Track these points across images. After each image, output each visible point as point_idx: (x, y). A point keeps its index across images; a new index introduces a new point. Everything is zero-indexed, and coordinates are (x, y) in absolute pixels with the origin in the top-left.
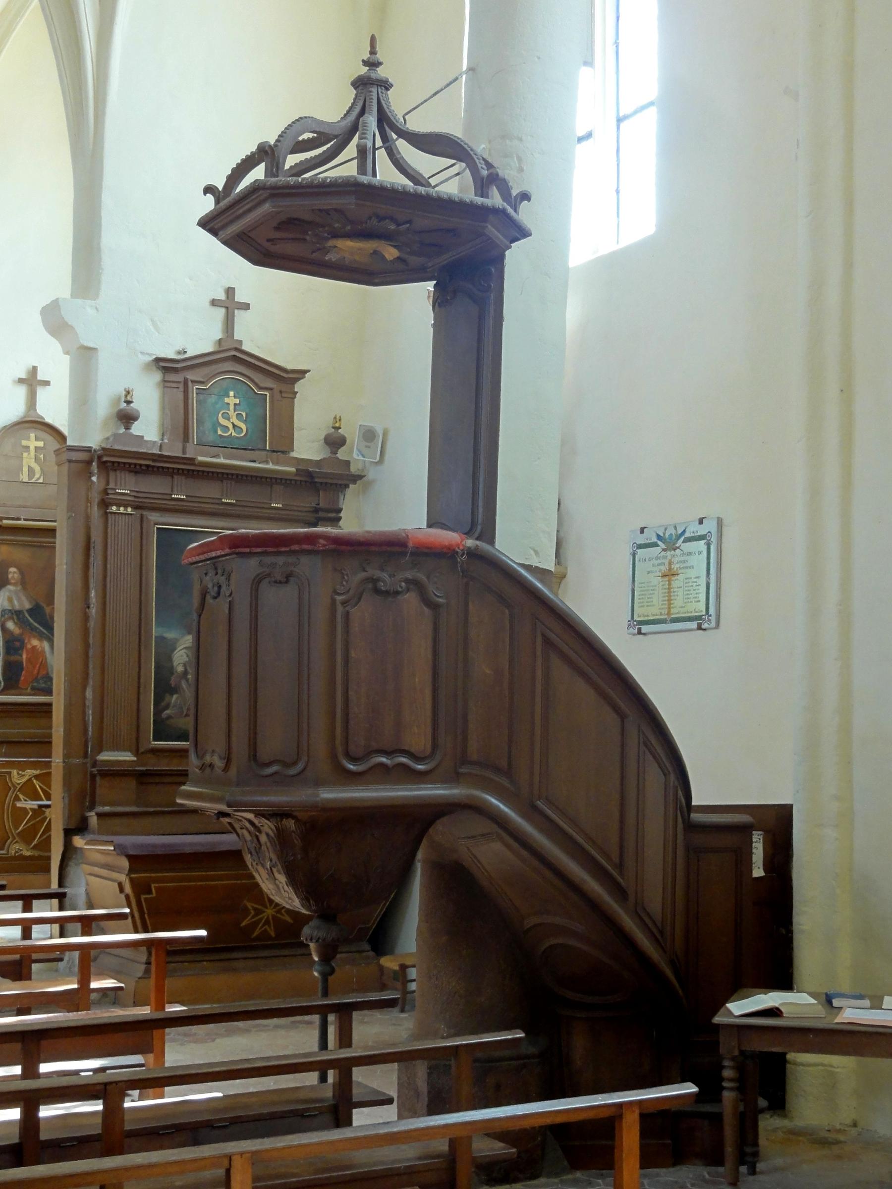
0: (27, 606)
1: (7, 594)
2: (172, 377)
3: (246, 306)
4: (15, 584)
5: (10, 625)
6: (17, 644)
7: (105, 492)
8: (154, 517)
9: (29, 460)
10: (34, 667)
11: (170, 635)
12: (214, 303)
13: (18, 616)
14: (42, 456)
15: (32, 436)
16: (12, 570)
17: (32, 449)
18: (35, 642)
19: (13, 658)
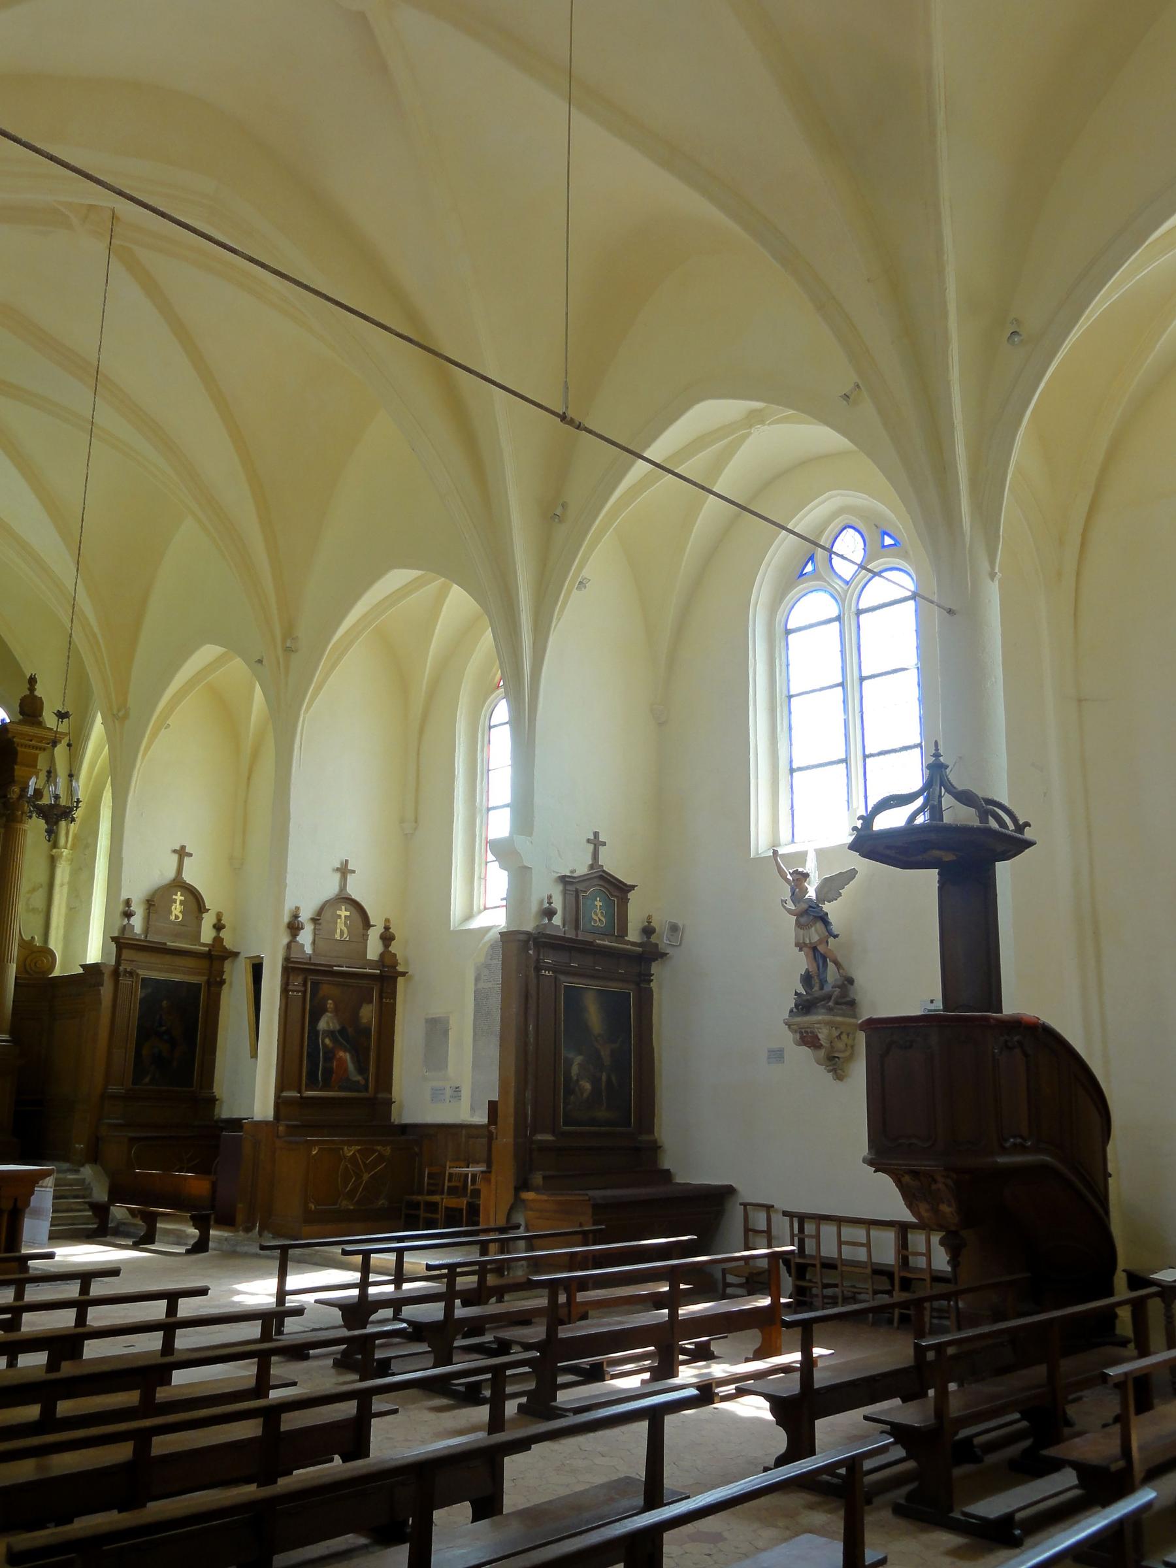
0: (338, 1027)
2: (569, 887)
3: (604, 844)
5: (327, 1041)
7: (538, 961)
8: (562, 978)
9: (341, 925)
11: (571, 1055)
12: (589, 841)
18: (341, 1054)
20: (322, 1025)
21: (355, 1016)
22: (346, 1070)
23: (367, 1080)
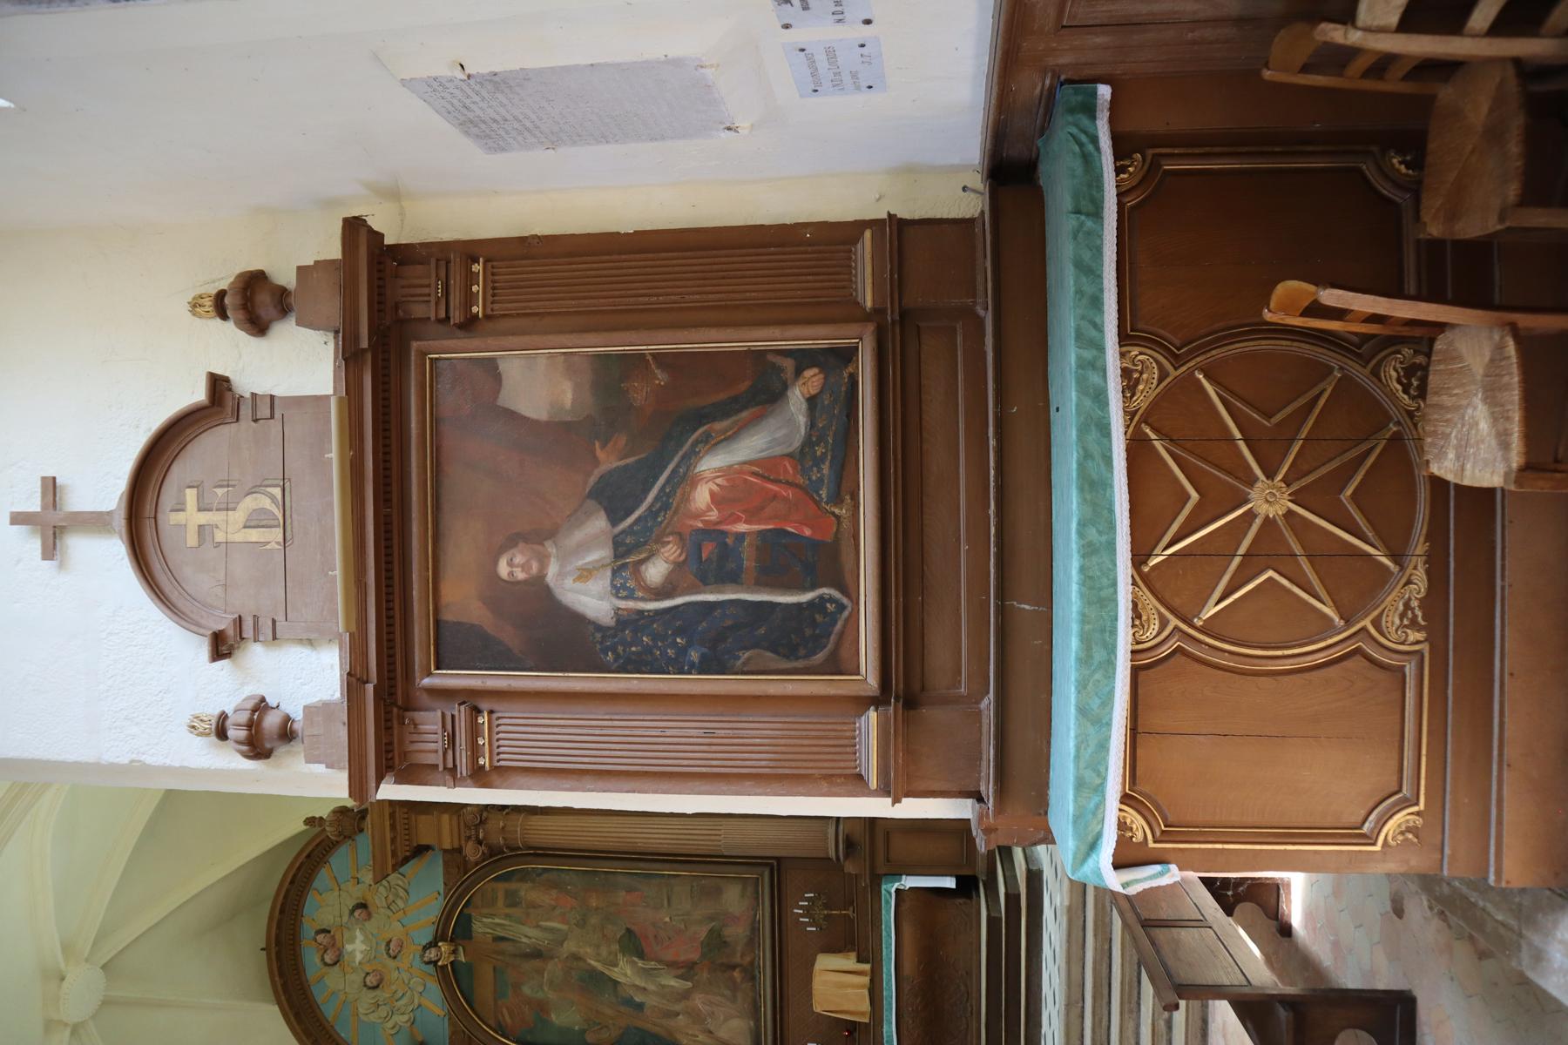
1: (569, 582)
4: (543, 560)
5: (656, 571)
6: (708, 549)
9: (231, 526)
10: (775, 496)
13: (628, 553)
14: (220, 491)
15: (176, 518)
16: (503, 569)
17: (204, 518)
18: (702, 496)
19: (748, 558)
20: (593, 599)
21: (560, 439)
22: (766, 468)
23: (804, 359)
